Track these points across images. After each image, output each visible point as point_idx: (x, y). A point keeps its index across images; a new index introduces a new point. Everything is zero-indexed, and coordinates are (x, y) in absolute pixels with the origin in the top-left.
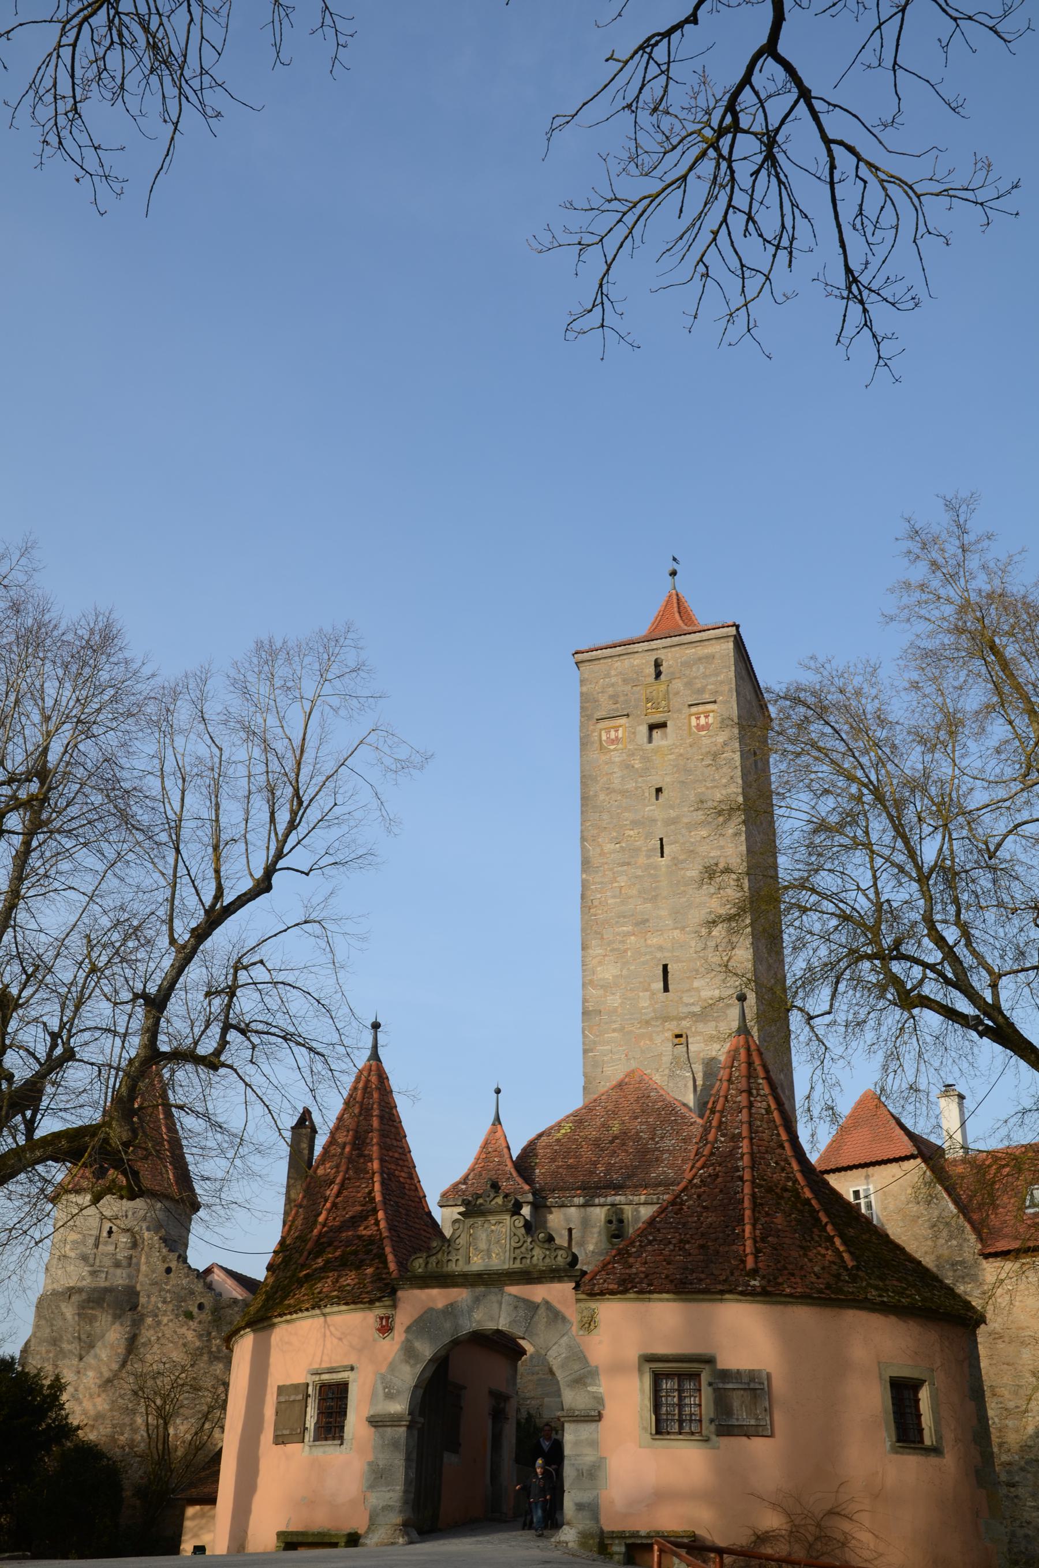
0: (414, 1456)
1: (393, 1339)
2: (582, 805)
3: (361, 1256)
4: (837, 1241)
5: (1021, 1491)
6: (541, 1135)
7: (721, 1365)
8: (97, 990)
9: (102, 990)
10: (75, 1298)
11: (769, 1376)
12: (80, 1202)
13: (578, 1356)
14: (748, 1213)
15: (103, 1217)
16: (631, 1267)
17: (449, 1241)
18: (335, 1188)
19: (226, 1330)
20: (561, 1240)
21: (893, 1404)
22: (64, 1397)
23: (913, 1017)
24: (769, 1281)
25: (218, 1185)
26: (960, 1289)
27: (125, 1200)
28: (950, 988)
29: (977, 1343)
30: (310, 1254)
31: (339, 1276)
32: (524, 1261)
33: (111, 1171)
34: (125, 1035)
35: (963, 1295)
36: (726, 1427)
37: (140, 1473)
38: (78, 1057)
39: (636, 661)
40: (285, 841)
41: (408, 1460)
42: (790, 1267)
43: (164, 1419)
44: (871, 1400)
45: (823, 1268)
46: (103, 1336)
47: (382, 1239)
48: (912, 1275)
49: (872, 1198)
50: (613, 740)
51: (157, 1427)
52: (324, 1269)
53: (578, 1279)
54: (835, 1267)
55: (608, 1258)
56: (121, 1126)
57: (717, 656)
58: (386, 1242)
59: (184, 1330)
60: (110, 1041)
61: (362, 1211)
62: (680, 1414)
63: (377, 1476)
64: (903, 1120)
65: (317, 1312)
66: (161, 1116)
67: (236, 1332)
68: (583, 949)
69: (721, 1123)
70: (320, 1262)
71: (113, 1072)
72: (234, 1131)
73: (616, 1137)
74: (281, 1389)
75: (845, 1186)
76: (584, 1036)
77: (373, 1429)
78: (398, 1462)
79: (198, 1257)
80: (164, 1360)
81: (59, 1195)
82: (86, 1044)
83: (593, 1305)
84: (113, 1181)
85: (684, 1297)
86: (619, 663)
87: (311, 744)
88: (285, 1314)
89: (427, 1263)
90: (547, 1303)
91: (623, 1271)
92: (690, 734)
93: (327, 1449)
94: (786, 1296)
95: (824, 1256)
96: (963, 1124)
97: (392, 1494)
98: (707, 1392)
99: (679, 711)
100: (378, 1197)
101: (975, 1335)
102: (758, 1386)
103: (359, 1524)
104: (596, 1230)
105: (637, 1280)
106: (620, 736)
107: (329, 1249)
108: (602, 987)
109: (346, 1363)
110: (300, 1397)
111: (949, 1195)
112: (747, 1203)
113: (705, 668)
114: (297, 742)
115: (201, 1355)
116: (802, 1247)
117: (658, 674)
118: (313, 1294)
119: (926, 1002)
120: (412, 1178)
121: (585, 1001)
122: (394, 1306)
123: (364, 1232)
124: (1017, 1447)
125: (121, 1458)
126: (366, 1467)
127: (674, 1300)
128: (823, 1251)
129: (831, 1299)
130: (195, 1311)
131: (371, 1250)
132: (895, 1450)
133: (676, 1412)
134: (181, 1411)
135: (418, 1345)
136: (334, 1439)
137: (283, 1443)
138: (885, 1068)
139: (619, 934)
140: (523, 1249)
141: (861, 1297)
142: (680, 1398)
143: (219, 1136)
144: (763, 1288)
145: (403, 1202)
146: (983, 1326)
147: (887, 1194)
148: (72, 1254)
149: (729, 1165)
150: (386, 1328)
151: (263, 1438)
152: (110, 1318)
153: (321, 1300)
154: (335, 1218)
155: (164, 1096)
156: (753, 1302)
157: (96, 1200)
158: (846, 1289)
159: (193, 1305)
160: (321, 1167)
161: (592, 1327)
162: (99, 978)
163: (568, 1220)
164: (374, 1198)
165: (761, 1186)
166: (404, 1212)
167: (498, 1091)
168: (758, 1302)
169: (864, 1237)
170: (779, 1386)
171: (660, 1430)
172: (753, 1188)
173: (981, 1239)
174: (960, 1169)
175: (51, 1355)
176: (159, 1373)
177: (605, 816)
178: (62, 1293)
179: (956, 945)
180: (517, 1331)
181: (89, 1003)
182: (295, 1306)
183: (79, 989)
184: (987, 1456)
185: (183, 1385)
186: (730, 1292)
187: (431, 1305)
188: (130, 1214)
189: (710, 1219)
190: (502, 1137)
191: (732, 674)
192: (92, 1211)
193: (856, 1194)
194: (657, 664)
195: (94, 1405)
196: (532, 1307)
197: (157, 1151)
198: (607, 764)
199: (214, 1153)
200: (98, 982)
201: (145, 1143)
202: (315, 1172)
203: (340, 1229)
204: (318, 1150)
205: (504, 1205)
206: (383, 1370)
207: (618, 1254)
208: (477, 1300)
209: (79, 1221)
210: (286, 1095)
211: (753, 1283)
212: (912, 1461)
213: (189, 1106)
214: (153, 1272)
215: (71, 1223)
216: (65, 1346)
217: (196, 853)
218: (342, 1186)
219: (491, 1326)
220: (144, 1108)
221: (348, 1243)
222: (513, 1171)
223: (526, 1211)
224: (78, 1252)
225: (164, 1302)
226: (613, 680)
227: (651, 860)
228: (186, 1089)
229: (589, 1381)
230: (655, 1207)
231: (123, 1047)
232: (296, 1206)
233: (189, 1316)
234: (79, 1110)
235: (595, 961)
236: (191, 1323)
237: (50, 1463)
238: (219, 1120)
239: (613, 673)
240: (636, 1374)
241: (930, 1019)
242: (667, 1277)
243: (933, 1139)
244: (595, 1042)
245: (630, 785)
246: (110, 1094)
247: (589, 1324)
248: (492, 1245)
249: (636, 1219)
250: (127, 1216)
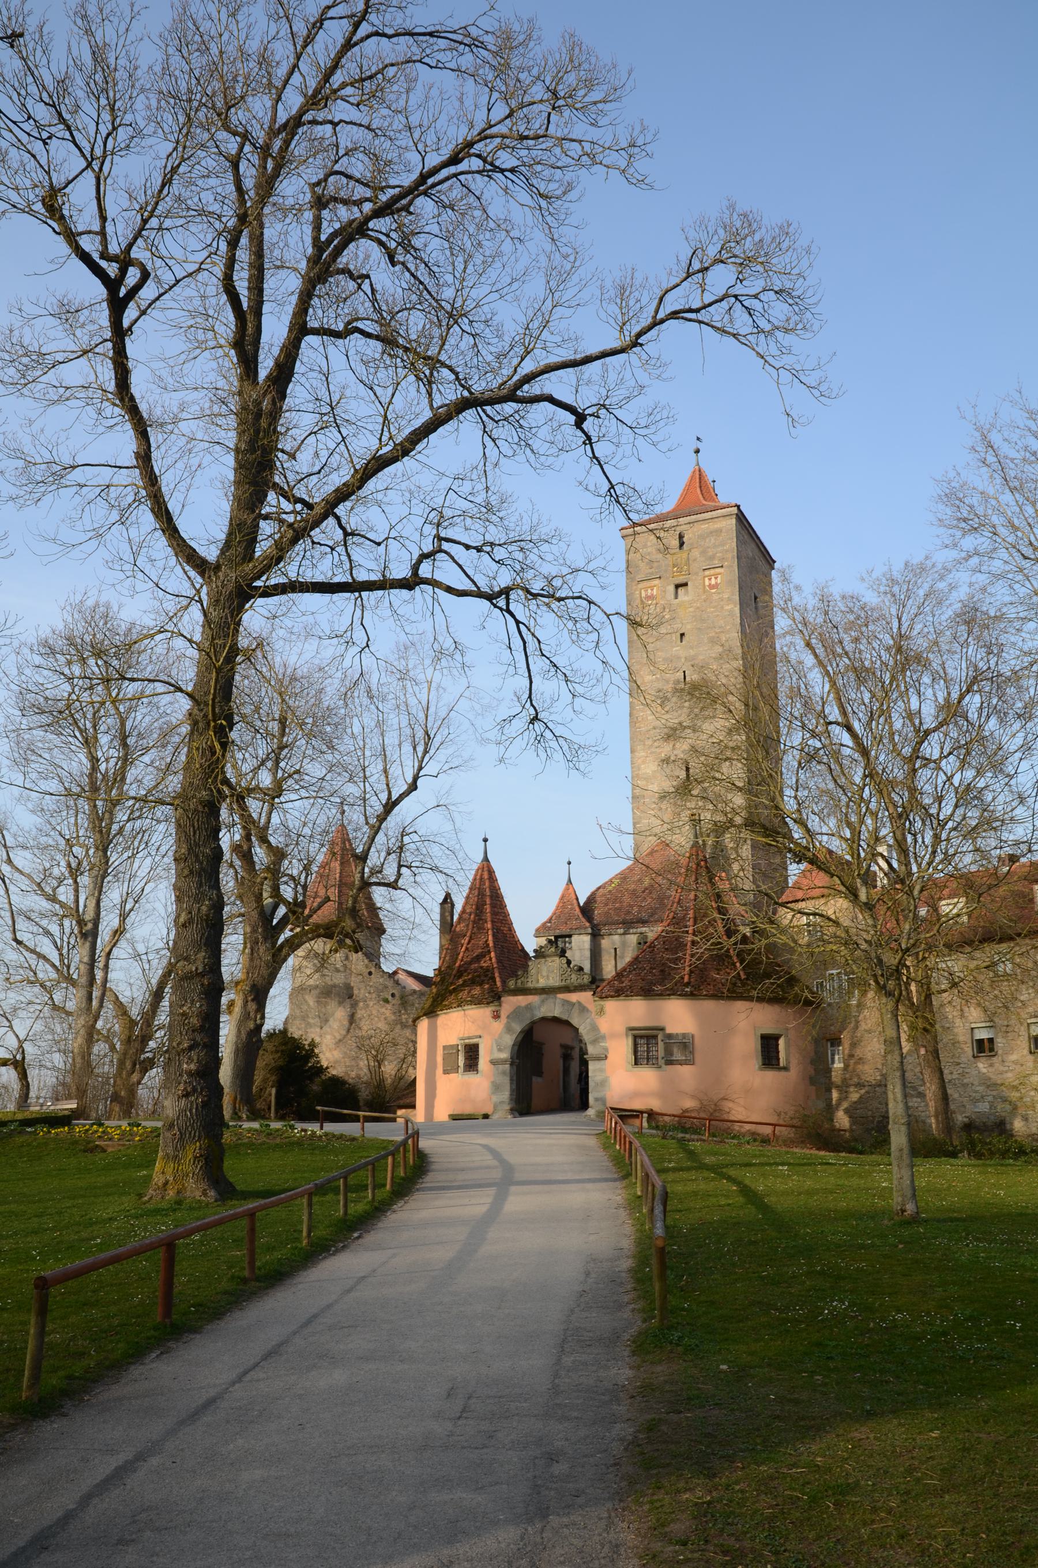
13: (595, 1028)
52: (463, 985)
63: (496, 1088)
70: (461, 981)
78: (506, 1081)
90: (579, 1003)
92: (705, 591)
97: (505, 1095)
99: (697, 574)
103: (488, 1110)
117: (682, 544)
132: (761, 1069)
150: (496, 1016)
163: (613, 943)
191: (734, 544)
194: (681, 537)
204: (456, 917)
217: (375, 769)
218: (471, 938)
219: (550, 1014)
221: (476, 971)
247: (601, 1012)
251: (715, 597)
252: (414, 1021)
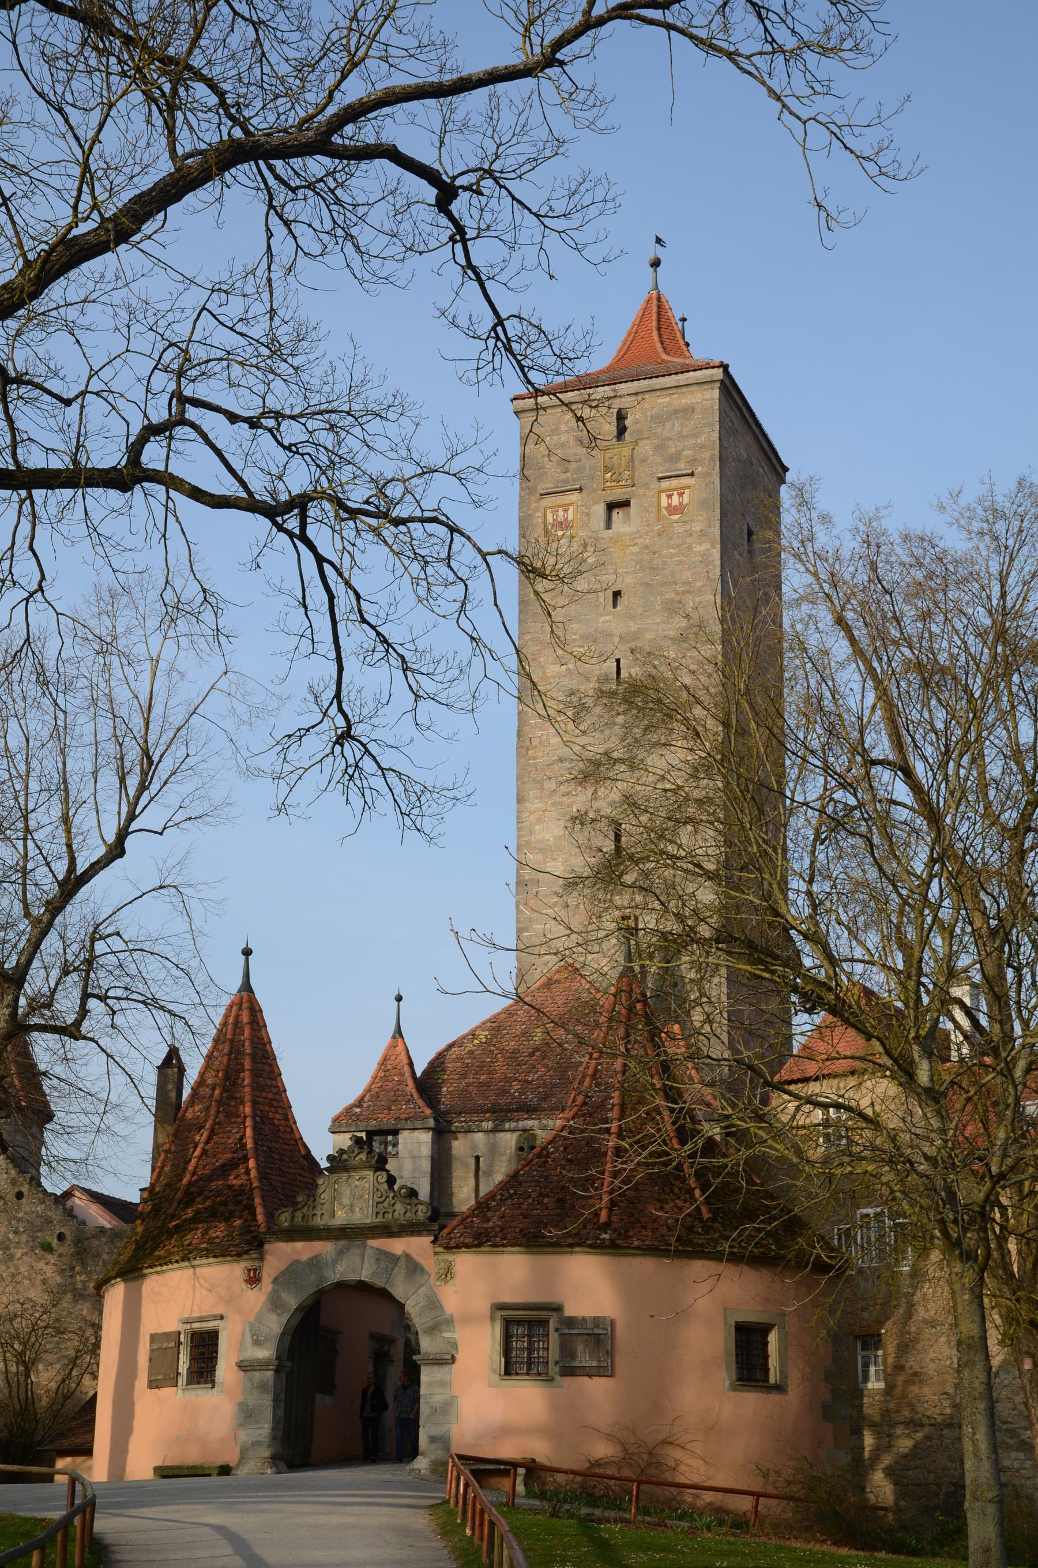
2: (520, 612)
3: (231, 1207)
6: (451, 1046)
13: (434, 1304)
18: (206, 1134)
21: (737, 1347)
31: (209, 1228)
40: (136, 804)
41: (276, 1400)
42: (643, 1220)
47: (252, 1189)
52: (193, 1220)
57: (698, 409)
58: (257, 1194)
63: (247, 1415)
68: (519, 801)
69: (596, 1071)
70: (190, 1213)
73: (537, 1049)
76: (519, 911)
78: (266, 1402)
83: (449, 1257)
87: (160, 699)
90: (407, 1256)
97: (263, 1429)
99: (646, 485)
100: (250, 1145)
103: (230, 1457)
104: (505, 1158)
106: (570, 517)
107: (198, 1199)
108: (541, 850)
109: (214, 1313)
113: (682, 425)
114: (144, 698)
116: (659, 1200)
117: (621, 431)
120: (287, 1119)
122: (262, 1259)
123: (234, 1182)
128: (680, 1203)
132: (734, 1388)
135: (284, 1295)
140: (385, 1204)
150: (253, 1279)
156: (602, 1254)
160: (191, 1110)
163: (474, 1147)
164: (245, 1145)
166: (277, 1157)
167: (399, 999)
168: (607, 1254)
186: (579, 1245)
187: (296, 1257)
190: (403, 1053)
191: (715, 436)
194: (621, 417)
203: (209, 1178)
204: (186, 1093)
205: (367, 1161)
206: (252, 1318)
208: (341, 1253)
210: (149, 1056)
211: (603, 1236)
218: (212, 1133)
219: (353, 1277)
221: (219, 1193)
222: (414, 1091)
226: (564, 438)
235: (533, 818)
239: (563, 428)
244: (531, 920)
247: (447, 1274)
251: (679, 529)
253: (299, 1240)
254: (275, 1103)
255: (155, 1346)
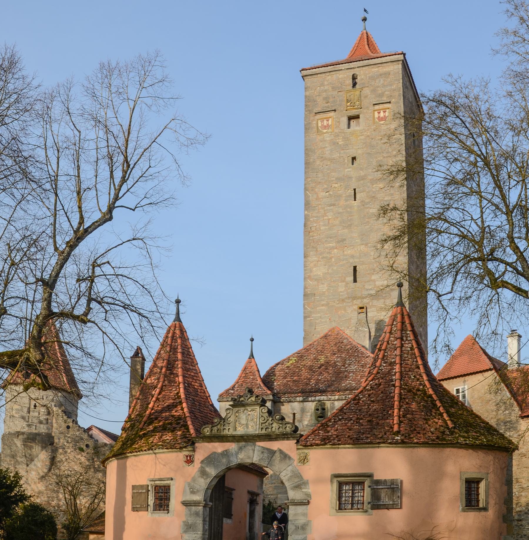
0: (207, 519)
1: (194, 466)
2: (305, 168)
4: (445, 415)
5: (524, 523)
7: (375, 478)
8: (16, 275)
9: (18, 276)
10: (21, 437)
11: (402, 482)
12: (18, 390)
13: (297, 475)
14: (396, 403)
15: (30, 398)
16: (329, 432)
17: (224, 419)
18: (158, 390)
19: (102, 458)
20: (289, 419)
22: (21, 482)
23: (498, 294)
24: (406, 437)
25: (91, 386)
26: (507, 434)
27: (41, 390)
28: (519, 276)
29: (512, 459)
30: (145, 423)
31: (162, 435)
32: (267, 429)
33: (32, 375)
34: (33, 302)
35: (508, 438)
36: (376, 504)
37: (64, 518)
38: (8, 313)
39: (341, 75)
43: (74, 496)
44: (452, 489)
45: (436, 429)
46: (37, 456)
47: (185, 418)
48: (483, 430)
49: (466, 392)
50: (325, 127)
51: (71, 499)
52: (153, 431)
53: (298, 438)
54: (442, 428)
55: (316, 428)
56: (35, 352)
57: (392, 73)
58: (188, 419)
59: (79, 456)
60: (25, 304)
61: (174, 402)
62: (352, 500)
64: (487, 351)
65: (151, 452)
66: (57, 348)
67: (108, 459)
68: (305, 257)
70: (151, 428)
71: (28, 322)
72: (99, 358)
74: (134, 487)
75: (451, 387)
76: (305, 308)
77: (185, 507)
79: (84, 421)
80: (70, 470)
81: (6, 385)
82: (12, 306)
83: (306, 451)
84: (34, 380)
85: (357, 446)
86: (330, 77)
88: (133, 452)
89: (212, 430)
91: (324, 434)
92: (374, 123)
93: (160, 514)
94: (414, 443)
95: (437, 423)
96: (519, 351)
98: (367, 491)
99: (368, 108)
101: (512, 455)
102: (395, 486)
105: (332, 438)
106: (330, 123)
108: (316, 280)
110: (144, 491)
111: (508, 388)
112: (396, 398)
113: (384, 81)
115: (90, 468)
116: (425, 419)
117: (354, 85)
118: (148, 443)
119: (505, 285)
121: (305, 288)
122: (194, 451)
123: (175, 414)
124: (525, 504)
125: (53, 511)
126: (182, 523)
127: (352, 448)
129: (439, 444)
130: (85, 448)
131: (180, 423)
133: (350, 499)
134: (82, 493)
135: (208, 469)
136: (164, 510)
137: (137, 511)
138: (480, 322)
139: (327, 248)
141: (455, 442)
142: (353, 493)
143: (89, 360)
144: (402, 440)
145: (197, 398)
146: (516, 451)
147: (476, 392)
148: (17, 415)
149: (388, 379)
151: (126, 508)
152: (40, 448)
153: (153, 446)
154: (158, 406)
155: (57, 336)
156: (396, 447)
157: (26, 389)
158: (447, 438)
159: (83, 445)
160: (149, 379)
161: (305, 462)
162: (16, 269)
164: (180, 396)
165: (405, 389)
166: (198, 404)
167: (252, 340)
169: (460, 412)
170: (406, 486)
171: (341, 508)
172: (400, 390)
173: (521, 409)
174: (515, 375)
175: (12, 462)
176: (68, 475)
177: (320, 175)
178: (14, 434)
179: (524, 251)
180: (263, 464)
181: (12, 283)
182: (139, 448)
183: (6, 275)
184: (510, 509)
185: (82, 482)
186: (384, 443)
187: (215, 450)
188: (45, 398)
189: (375, 407)
192: (24, 394)
193: (458, 391)
194: (354, 78)
195: (37, 487)
196: (272, 453)
197: (56, 366)
198: (321, 141)
199: (87, 369)
200: (16, 271)
201: (49, 361)
202: (146, 382)
203: (161, 411)
204: (147, 370)
207: (322, 426)
208: (240, 449)
209: (18, 399)
211: (396, 438)
212: (472, 516)
213: (72, 343)
214: (60, 427)
215: (14, 400)
216: (19, 459)
218: (162, 389)
219: (249, 461)
220: (47, 343)
221: (167, 419)
223: (269, 404)
224: (19, 414)
225: (68, 442)
226: (326, 88)
227: (348, 203)
228: (70, 333)
229: (303, 487)
230: (344, 402)
231: (33, 309)
232: (136, 399)
233: (82, 450)
234: (12, 342)
235: (312, 265)
236: (83, 453)
237: (19, 510)
238: (89, 351)
239: (326, 83)
240: (330, 483)
241: (507, 294)
242: (349, 436)
243: (503, 360)
245: (336, 155)
246: (28, 334)
247: (304, 460)
248: (250, 420)
249: (333, 408)
250: (43, 399)
252: (103, 462)
253: (216, 442)
254: (195, 378)
255: (135, 491)
